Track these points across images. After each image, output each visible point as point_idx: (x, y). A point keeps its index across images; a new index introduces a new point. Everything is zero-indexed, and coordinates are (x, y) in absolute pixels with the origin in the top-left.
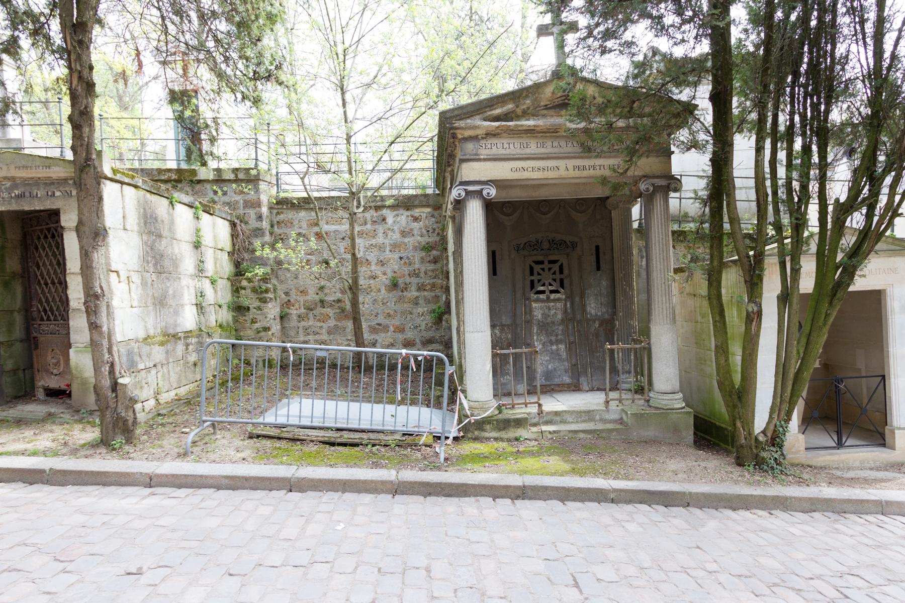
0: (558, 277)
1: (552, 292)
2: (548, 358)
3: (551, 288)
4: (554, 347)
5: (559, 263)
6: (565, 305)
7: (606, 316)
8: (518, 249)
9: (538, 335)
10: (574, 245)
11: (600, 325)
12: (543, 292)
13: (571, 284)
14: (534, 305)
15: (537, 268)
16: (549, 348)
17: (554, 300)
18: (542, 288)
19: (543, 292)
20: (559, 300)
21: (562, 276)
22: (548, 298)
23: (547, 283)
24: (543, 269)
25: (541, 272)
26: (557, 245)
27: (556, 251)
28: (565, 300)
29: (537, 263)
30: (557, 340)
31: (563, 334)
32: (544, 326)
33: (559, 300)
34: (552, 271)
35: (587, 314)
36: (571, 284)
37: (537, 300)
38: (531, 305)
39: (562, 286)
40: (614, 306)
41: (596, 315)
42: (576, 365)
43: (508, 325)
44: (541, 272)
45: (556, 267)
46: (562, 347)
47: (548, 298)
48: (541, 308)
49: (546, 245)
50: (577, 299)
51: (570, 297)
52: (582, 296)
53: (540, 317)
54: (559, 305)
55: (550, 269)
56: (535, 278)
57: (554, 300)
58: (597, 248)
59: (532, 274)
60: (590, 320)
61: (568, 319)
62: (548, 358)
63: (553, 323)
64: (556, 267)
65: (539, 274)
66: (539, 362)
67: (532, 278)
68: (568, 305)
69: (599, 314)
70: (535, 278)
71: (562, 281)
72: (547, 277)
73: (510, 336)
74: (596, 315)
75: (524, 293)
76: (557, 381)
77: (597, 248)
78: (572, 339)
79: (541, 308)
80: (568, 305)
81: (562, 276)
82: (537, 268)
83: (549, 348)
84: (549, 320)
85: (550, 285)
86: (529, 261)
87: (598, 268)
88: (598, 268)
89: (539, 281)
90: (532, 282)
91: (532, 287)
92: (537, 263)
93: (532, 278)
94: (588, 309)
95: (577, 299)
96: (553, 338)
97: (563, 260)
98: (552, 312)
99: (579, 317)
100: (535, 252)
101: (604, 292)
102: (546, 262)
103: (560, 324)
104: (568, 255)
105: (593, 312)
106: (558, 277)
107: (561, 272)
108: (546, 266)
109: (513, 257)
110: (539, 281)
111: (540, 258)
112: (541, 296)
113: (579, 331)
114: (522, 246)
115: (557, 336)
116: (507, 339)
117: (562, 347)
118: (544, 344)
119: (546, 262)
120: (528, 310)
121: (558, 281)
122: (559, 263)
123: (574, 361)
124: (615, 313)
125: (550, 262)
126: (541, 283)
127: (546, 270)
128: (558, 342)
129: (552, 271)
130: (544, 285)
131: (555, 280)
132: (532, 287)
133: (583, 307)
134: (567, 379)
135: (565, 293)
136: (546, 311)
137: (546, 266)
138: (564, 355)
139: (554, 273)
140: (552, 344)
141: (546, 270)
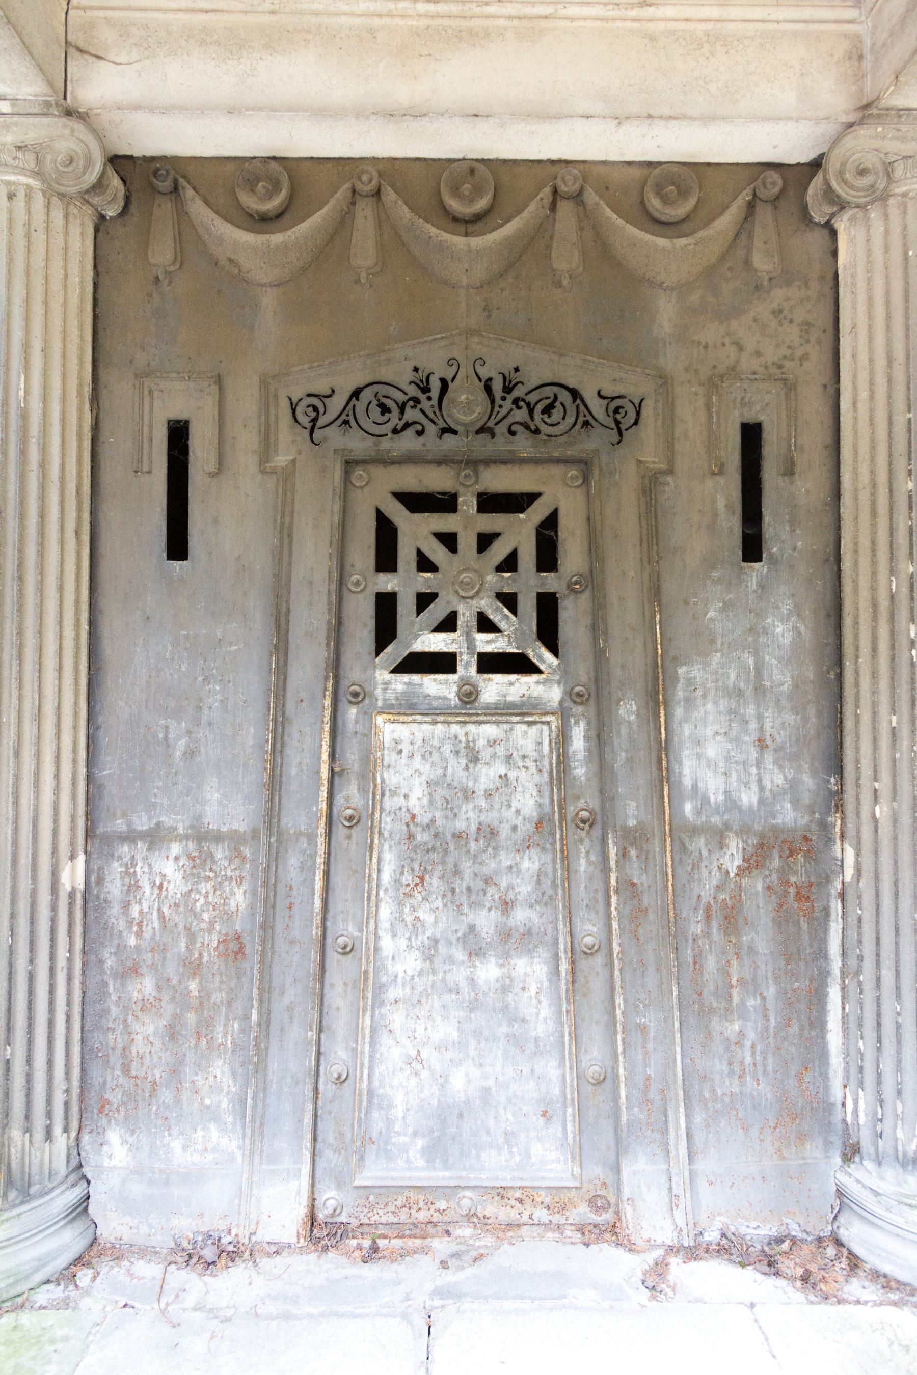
0: (528, 582)
1: (491, 663)
2: (447, 1030)
3: (487, 643)
4: (489, 971)
5: (536, 514)
6: (563, 738)
7: (788, 815)
8: (311, 416)
9: (404, 895)
10: (622, 417)
11: (753, 863)
12: (443, 663)
13: (598, 626)
14: (389, 731)
15: (416, 532)
16: (459, 975)
17: (505, 711)
18: (437, 643)
19: (443, 663)
20: (524, 711)
21: (551, 582)
22: (469, 696)
23: (467, 616)
24: (449, 541)
25: (437, 553)
26: (529, 407)
27: (523, 444)
28: (563, 713)
29: (417, 502)
30: (505, 935)
31: (543, 900)
32: (443, 853)
33: (524, 711)
34: (499, 552)
35: (676, 800)
36: (598, 626)
37: (408, 708)
38: (368, 733)
39: (548, 633)
40: (835, 762)
41: (731, 803)
42: (606, 1081)
43: (235, 840)
44: (437, 553)
45: (519, 533)
46: (532, 970)
47: (469, 696)
48: (428, 751)
49: (467, 404)
50: (628, 710)
51: (591, 698)
52: (657, 696)
53: (417, 799)
54: (530, 738)
55: (485, 541)
56: (404, 583)
57: (505, 711)
58: (751, 435)
59: (386, 561)
60: (695, 831)
61: (575, 819)
62: (447, 1030)
63: (488, 833)
64: (519, 533)
65: (425, 564)
66: (392, 1052)
67: (388, 583)
68: (578, 742)
69: (748, 798)
70: (404, 583)
71: (548, 606)
72: (468, 585)
73: (239, 899)
74: (731, 803)
75: (335, 666)
76: (494, 1166)
77: (751, 435)
78: (589, 931)
79: (428, 751)
80: (578, 742)
81: (551, 582)
82: (416, 532)
83: (459, 975)
84: (468, 817)
85: (485, 625)
86: (377, 491)
87: (752, 548)
88: (752, 548)
89: (424, 601)
90: (386, 605)
91: (385, 630)
92: (417, 502)
93: (388, 583)
94: (688, 769)
95: (628, 710)
96: (486, 921)
97: (558, 492)
98: (487, 775)
99: (632, 811)
100: (408, 442)
101: (780, 677)
102: (468, 503)
103: (525, 846)
104: (585, 465)
105: (714, 786)
106: (528, 582)
107: (547, 558)
108: (467, 521)
109: (281, 460)
110: (424, 601)
111: (436, 480)
112: (434, 685)
113: (629, 888)
114: (336, 405)
115: (506, 906)
116: (227, 916)
117: (532, 970)
118: (431, 950)
119: (468, 503)
120: (351, 756)
121: (528, 605)
122: (536, 514)
123: (594, 1058)
124: (835, 800)
125: (491, 503)
126: (437, 612)
127: (467, 542)
128: (511, 941)
129: (499, 552)
130: (448, 624)
131: (509, 601)
132: (385, 630)
133: (661, 754)
134: (549, 1160)
135: (565, 673)
136: (456, 767)
137: (467, 521)
138: (541, 1016)
139: (510, 564)
140: (476, 953)
141: (467, 542)
